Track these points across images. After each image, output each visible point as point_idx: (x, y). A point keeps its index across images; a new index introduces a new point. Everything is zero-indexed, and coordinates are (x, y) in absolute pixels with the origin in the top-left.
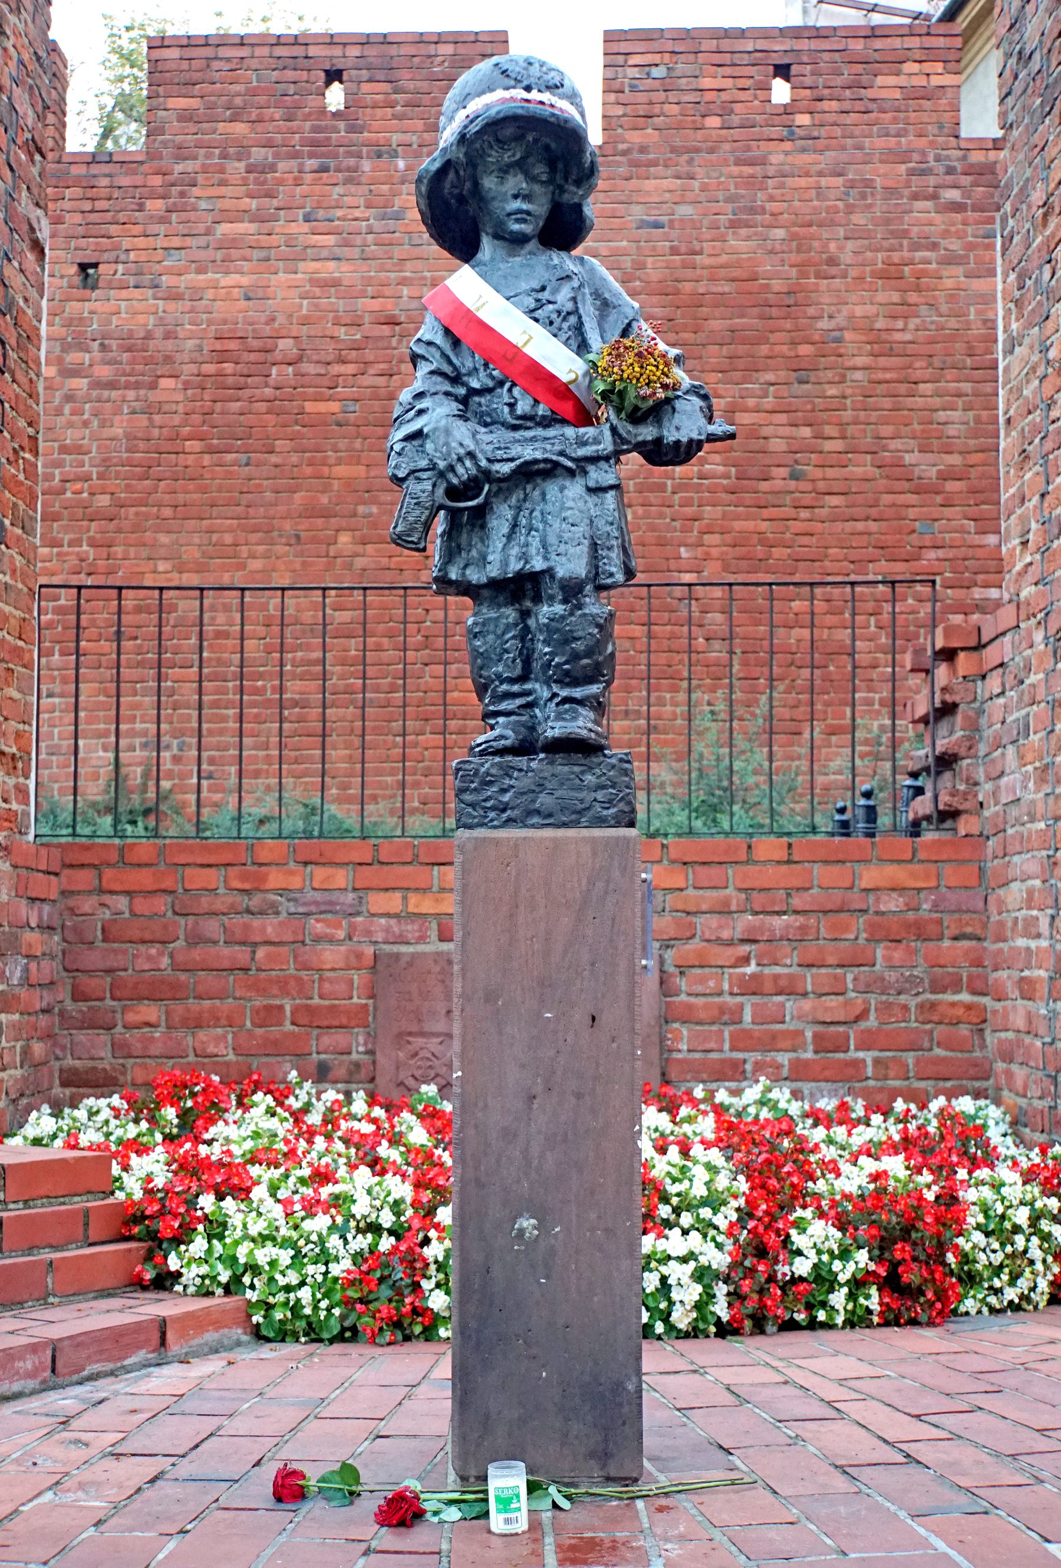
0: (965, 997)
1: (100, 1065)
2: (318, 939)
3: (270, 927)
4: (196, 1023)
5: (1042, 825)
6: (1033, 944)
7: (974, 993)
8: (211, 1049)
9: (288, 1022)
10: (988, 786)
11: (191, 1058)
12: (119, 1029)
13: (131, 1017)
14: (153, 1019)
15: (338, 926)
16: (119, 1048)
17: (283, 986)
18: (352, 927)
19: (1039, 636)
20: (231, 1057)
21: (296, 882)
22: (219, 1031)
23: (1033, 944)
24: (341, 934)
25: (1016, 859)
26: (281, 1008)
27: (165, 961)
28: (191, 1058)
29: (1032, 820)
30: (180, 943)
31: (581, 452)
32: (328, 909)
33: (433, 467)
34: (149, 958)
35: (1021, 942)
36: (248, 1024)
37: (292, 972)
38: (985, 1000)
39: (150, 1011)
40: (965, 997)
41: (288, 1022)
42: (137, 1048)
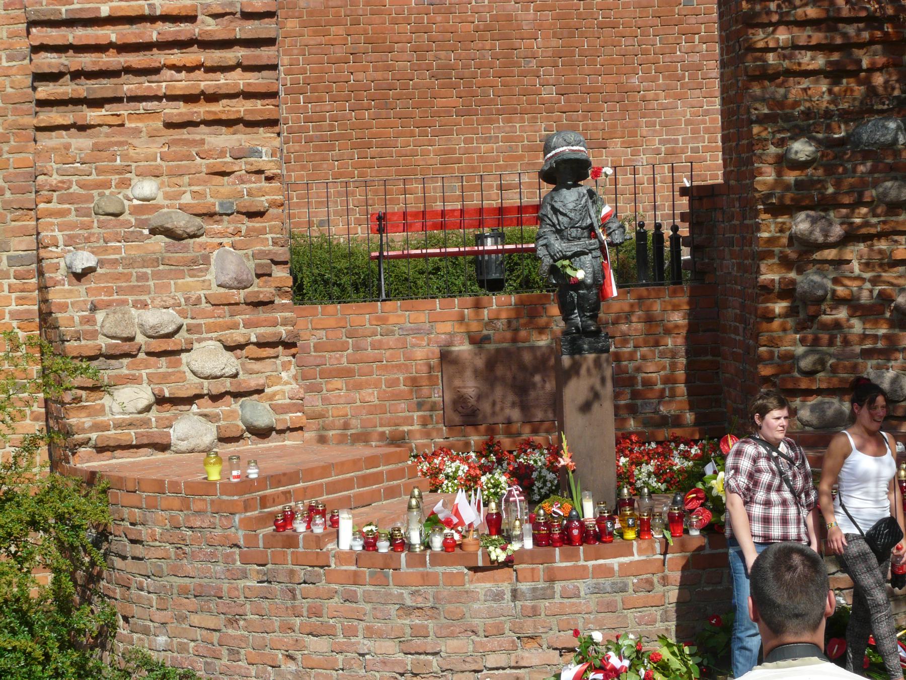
0: (709, 358)
1: (316, 409)
2: (413, 346)
3: (391, 341)
4: (359, 387)
5: (739, 288)
6: (738, 338)
7: (714, 356)
8: (367, 399)
9: (402, 385)
10: (718, 261)
11: (358, 404)
12: (324, 392)
13: (330, 386)
14: (339, 387)
15: (423, 340)
16: (325, 400)
17: (399, 367)
18: (429, 339)
19: (737, 205)
20: (377, 402)
21: (401, 320)
22: (370, 391)
23: (738, 338)
24: (425, 343)
25: (730, 298)
26: (398, 379)
27: (344, 360)
28: (358, 404)
29: (736, 284)
30: (350, 351)
31: (591, 247)
32: (417, 332)
33: (550, 254)
34: (337, 359)
35: (733, 336)
36: (384, 386)
37: (402, 361)
38: (719, 359)
39: (338, 383)
40: (709, 358)
41: (402, 385)
42: (333, 400)
